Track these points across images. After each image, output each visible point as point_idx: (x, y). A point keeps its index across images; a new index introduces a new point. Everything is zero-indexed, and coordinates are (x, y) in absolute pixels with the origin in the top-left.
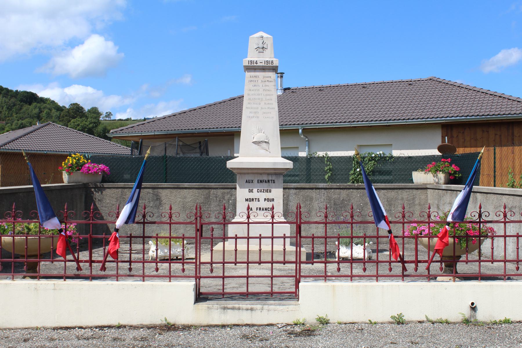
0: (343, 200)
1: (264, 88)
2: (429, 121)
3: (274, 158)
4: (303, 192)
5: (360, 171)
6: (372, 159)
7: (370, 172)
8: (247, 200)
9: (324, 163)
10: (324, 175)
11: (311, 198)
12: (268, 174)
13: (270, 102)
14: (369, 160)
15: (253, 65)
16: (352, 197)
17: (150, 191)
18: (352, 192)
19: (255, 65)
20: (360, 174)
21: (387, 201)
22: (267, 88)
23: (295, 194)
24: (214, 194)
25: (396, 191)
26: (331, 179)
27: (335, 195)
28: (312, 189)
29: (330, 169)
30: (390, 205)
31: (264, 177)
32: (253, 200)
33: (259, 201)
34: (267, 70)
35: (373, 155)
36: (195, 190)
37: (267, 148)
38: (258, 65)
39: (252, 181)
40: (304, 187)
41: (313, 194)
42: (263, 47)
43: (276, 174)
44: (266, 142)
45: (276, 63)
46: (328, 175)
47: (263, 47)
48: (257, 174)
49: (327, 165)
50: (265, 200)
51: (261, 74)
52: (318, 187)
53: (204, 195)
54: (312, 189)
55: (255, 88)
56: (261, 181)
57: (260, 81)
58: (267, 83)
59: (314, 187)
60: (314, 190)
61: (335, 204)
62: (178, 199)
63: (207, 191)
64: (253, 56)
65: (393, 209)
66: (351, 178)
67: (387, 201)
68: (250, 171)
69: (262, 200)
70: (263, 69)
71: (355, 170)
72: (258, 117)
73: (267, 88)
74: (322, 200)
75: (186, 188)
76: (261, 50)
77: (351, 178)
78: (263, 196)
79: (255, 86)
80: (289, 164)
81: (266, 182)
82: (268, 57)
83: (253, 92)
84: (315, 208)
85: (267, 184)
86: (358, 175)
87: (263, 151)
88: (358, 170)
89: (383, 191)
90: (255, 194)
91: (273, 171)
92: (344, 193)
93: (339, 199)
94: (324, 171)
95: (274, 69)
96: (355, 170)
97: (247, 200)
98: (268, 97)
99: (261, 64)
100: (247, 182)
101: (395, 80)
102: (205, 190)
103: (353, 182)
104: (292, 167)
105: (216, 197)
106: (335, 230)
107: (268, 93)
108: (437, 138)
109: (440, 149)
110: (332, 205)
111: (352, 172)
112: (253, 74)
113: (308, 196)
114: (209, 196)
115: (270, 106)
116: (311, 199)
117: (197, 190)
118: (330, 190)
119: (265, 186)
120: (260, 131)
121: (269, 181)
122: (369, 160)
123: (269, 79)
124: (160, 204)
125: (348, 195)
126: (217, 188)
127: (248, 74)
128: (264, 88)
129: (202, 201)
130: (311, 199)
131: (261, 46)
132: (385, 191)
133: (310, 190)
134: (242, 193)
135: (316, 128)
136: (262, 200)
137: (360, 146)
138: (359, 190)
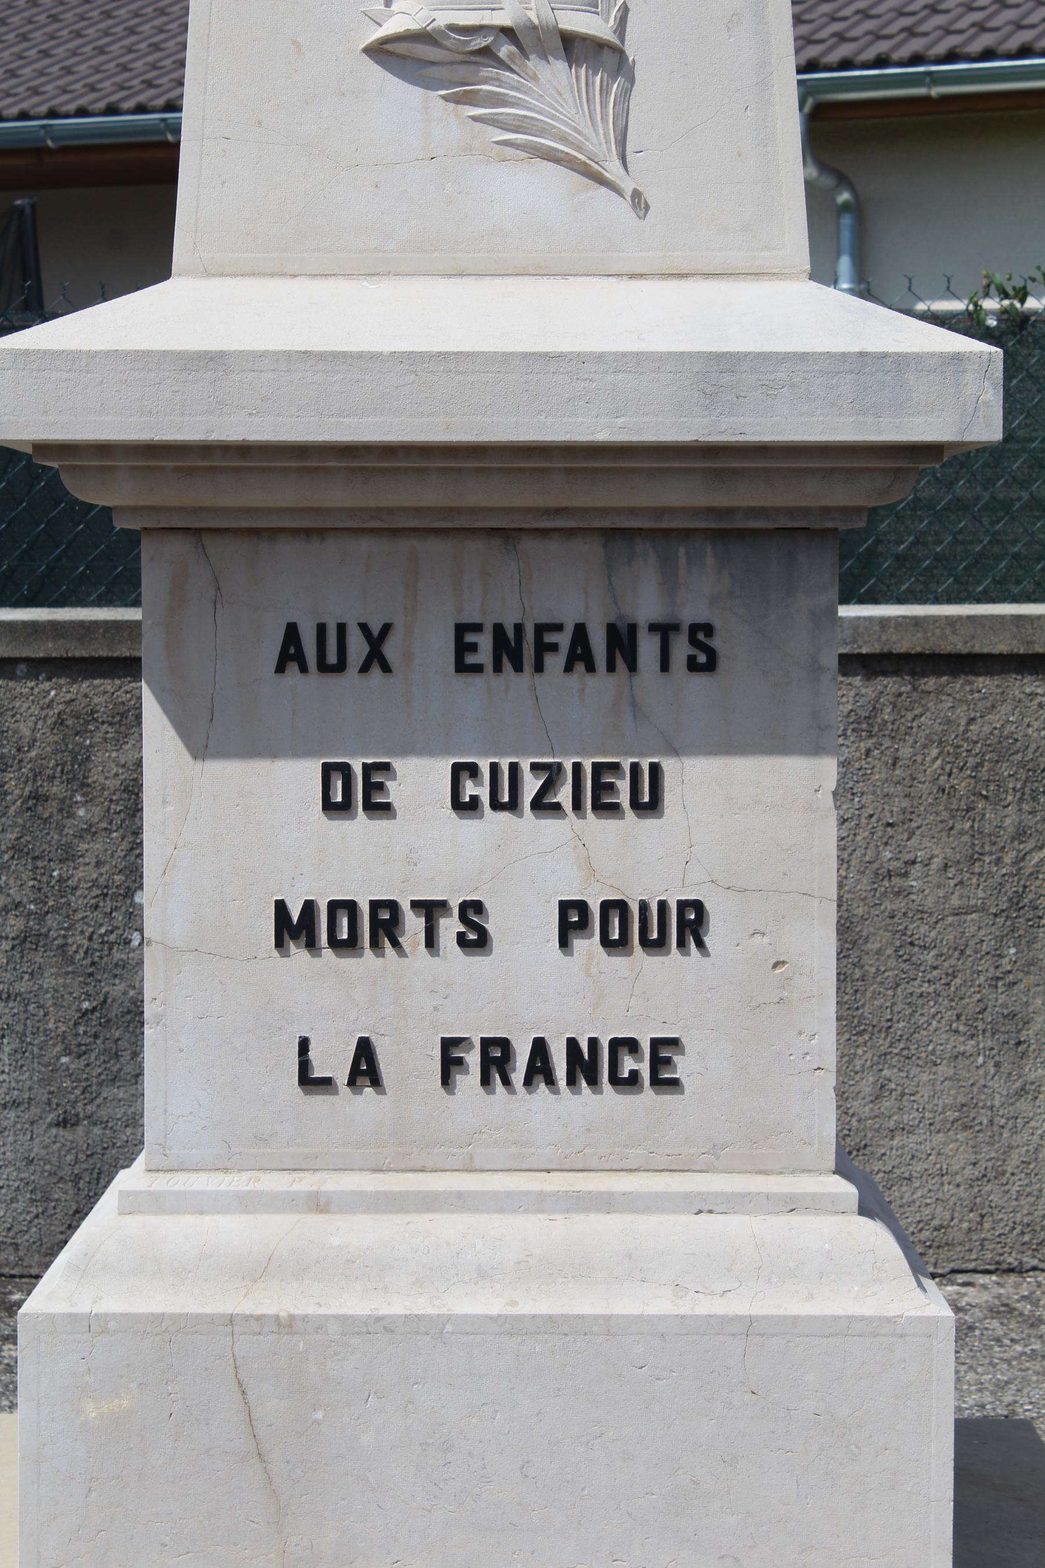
4: (948, 702)
8: (293, 928)
12: (619, 537)
23: (864, 723)
31: (563, 577)
32: (386, 922)
33: (476, 940)
37: (599, 145)
39: (376, 641)
40: (957, 644)
43: (728, 535)
44: (572, 47)
50: (572, 919)
56: (508, 650)
68: (337, 495)
69: (524, 924)
81: (580, 655)
85: (602, 685)
90: (423, 840)
97: (293, 928)
100: (291, 652)
104: (988, 427)
113: (1001, 747)
119: (570, 714)
121: (622, 643)
134: (221, 827)
135: (926, 100)
136: (524, 924)
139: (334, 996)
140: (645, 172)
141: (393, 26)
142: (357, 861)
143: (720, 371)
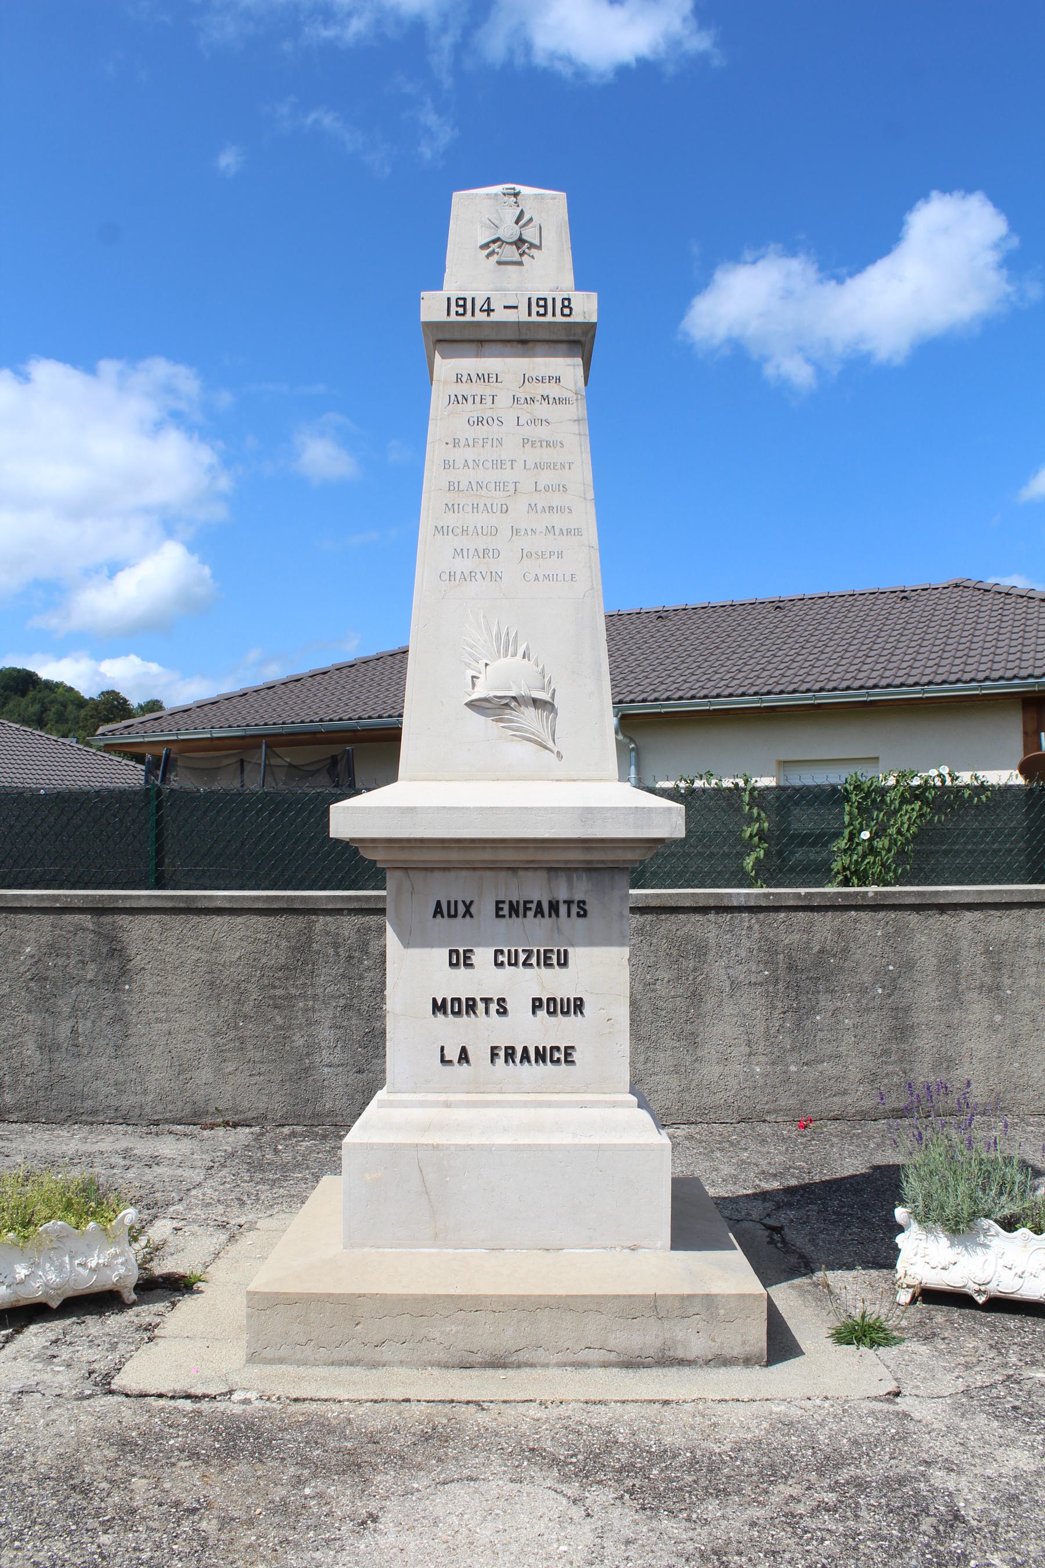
0: (822, 951)
1: (527, 431)
2: (990, 688)
3: (581, 786)
4: (670, 923)
5: (871, 839)
6: (918, 794)
7: (908, 842)
8: (439, 1007)
9: (740, 809)
10: (741, 856)
11: (699, 948)
12: (552, 870)
13: (556, 499)
14: (904, 801)
15: (468, 318)
16: (856, 939)
17: (86, 920)
18: (856, 921)
19: (480, 317)
20: (872, 850)
21: (987, 951)
22: (542, 432)
23: (640, 931)
24: (328, 933)
25: (1016, 913)
26: (767, 874)
27: (789, 932)
28: (704, 910)
29: (760, 832)
30: (997, 967)
31: (531, 886)
32: (471, 1006)
33: (503, 1012)
34: (539, 347)
35: (916, 782)
36: (254, 919)
37: (546, 737)
38: (494, 317)
39: (468, 907)
41: (709, 929)
42: (520, 242)
43: (591, 869)
44: (536, 702)
45: (586, 307)
46: (753, 856)
47: (520, 242)
48: (493, 867)
49: (750, 820)
50: (537, 1004)
51: (509, 367)
52: (726, 903)
53: (288, 940)
54: (704, 910)
55: (482, 431)
56: (514, 910)
57: (504, 400)
58: (541, 410)
59: (712, 903)
60: (712, 916)
61: (791, 968)
62: (191, 952)
63: (300, 922)
64: (467, 276)
65: (1007, 981)
66: (836, 866)
67: (987, 951)
68: (454, 856)
70: (521, 339)
71: (852, 837)
72: (495, 576)
73: (542, 432)
74: (743, 954)
75: (219, 911)
76: (511, 253)
77: (836, 866)
78: (525, 984)
79: (479, 421)
80: (668, 821)
81: (539, 911)
82: (549, 276)
83: (470, 454)
84: (715, 983)
85: (547, 922)
86: (864, 856)
87: (525, 751)
88: (865, 835)
89: (968, 915)
90: (483, 978)
91: (576, 856)
92: (825, 925)
93: (807, 948)
94: (740, 839)
95: (576, 340)
96: (852, 837)
97: (439, 1007)
98: (547, 478)
99: (511, 316)
100: (438, 911)
101: (858, 591)
102: (291, 919)
103: (846, 882)
104: (681, 833)
105: (336, 946)
106: (793, 1068)
107: (546, 455)
108: (1009, 735)
109: (1025, 769)
110: (781, 973)
111: (843, 843)
112: (469, 364)
113: (688, 939)
114: (310, 941)
115: (558, 520)
116: (701, 951)
117: (264, 919)
118: (773, 915)
119: (536, 932)
120: (506, 645)
121: (554, 907)
122: (904, 801)
123: (552, 390)
124: (124, 971)
125: (840, 932)
126: (339, 911)
127: (445, 367)
128: (527, 431)
129: (282, 961)
130: (701, 951)
131: (509, 231)
132: (978, 915)
133: (698, 917)
134: (413, 971)
135: (660, 713)
137: (784, 764)
138: (882, 914)
139: (454, 1031)
140: (562, 743)
141: (475, 696)
142: (461, 984)
143: (587, 813)
